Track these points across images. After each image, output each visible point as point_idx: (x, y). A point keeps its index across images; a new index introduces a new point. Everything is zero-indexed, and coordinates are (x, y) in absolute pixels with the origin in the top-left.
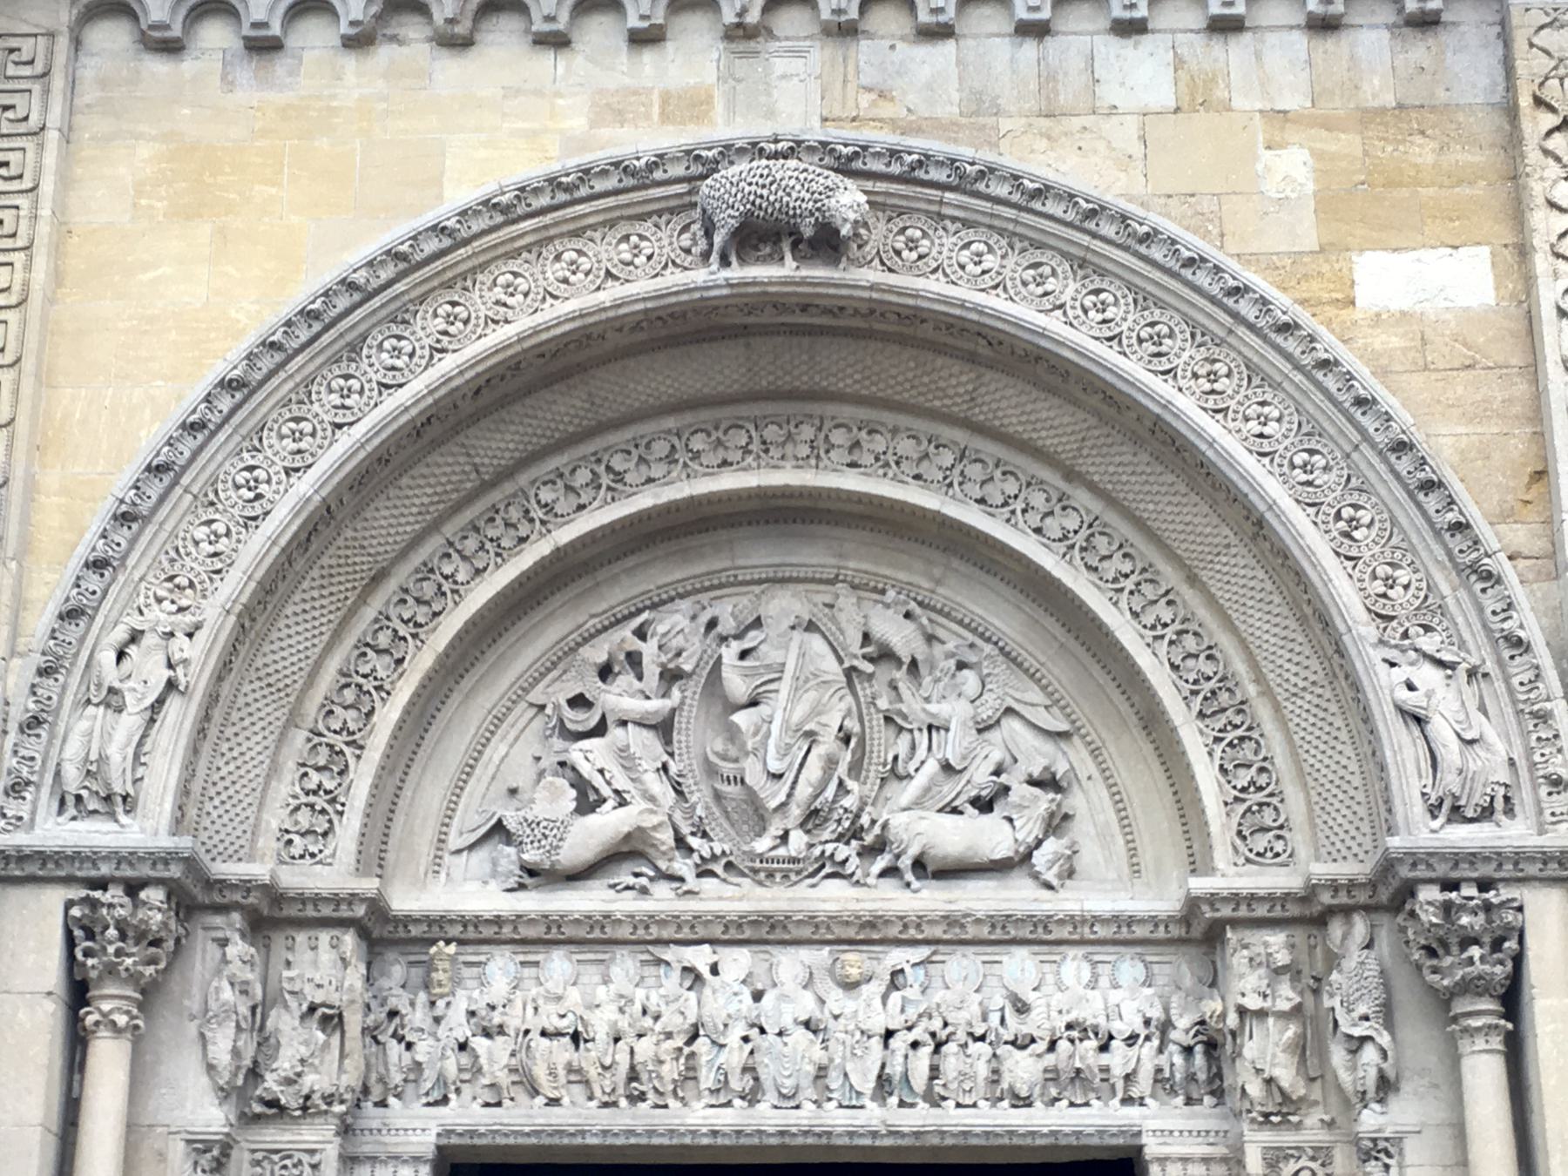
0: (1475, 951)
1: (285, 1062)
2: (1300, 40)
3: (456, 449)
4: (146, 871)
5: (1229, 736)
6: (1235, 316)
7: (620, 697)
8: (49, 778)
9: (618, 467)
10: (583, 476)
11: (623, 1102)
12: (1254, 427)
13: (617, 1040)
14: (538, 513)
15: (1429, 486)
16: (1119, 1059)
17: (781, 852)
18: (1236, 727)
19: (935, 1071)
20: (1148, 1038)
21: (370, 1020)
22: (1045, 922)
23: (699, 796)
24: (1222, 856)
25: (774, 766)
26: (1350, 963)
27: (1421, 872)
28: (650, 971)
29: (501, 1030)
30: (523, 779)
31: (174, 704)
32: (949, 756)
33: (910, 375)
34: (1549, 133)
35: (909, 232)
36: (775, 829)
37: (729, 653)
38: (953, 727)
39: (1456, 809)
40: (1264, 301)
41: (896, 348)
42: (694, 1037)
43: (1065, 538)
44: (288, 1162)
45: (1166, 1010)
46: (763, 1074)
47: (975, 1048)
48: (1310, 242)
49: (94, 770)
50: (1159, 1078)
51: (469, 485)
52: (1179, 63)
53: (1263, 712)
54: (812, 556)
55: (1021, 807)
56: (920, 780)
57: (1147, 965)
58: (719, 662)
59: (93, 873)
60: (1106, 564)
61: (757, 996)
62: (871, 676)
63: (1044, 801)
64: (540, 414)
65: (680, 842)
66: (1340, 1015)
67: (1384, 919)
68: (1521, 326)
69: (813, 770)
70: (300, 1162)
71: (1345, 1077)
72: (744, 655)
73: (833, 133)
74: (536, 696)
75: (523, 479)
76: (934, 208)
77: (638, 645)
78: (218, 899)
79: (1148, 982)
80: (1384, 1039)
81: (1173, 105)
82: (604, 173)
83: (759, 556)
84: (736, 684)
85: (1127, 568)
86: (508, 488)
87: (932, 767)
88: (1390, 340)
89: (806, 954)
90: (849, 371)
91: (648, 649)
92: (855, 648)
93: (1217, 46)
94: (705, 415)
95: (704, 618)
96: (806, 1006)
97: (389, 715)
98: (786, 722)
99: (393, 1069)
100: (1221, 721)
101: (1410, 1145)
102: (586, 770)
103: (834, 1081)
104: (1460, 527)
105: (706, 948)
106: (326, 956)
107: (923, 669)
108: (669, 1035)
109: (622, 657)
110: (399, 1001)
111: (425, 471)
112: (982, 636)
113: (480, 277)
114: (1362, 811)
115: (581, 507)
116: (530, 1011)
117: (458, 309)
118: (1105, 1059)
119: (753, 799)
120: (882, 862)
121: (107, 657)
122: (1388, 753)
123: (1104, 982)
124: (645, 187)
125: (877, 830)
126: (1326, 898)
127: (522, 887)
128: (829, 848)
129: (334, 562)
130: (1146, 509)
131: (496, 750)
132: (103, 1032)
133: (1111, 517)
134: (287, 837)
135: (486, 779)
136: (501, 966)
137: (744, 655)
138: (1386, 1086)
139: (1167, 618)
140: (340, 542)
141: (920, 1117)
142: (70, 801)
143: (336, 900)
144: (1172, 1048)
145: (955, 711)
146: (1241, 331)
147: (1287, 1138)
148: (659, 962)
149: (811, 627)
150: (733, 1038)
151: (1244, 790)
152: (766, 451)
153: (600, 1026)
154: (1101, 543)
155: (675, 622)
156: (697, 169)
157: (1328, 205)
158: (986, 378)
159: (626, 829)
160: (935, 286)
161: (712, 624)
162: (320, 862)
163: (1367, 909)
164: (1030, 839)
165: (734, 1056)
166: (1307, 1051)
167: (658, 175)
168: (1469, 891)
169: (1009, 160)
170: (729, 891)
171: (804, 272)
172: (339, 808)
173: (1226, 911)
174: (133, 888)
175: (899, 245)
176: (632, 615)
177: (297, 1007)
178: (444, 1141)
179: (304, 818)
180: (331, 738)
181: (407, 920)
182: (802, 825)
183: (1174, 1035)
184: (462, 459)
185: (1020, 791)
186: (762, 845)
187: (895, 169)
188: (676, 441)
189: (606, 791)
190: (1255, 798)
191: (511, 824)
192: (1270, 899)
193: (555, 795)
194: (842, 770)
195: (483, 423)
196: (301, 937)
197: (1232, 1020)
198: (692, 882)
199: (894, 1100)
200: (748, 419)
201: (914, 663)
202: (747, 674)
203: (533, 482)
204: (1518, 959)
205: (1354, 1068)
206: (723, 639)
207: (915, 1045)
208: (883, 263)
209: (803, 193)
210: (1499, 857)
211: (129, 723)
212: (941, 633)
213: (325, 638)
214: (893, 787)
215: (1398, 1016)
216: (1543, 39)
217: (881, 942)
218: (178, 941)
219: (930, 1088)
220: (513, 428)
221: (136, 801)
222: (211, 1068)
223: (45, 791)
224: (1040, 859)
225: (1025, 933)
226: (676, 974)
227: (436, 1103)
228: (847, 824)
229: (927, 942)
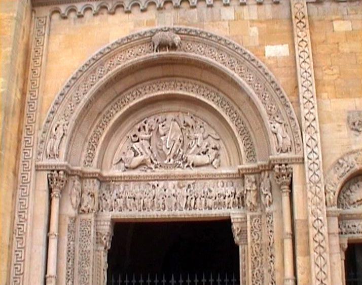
0: (284, 177)
1: (85, 204)
2: (256, 7)
5: (246, 138)
6: (244, 58)
7: (142, 135)
11: (142, 210)
12: (248, 79)
13: (141, 199)
15: (278, 89)
16: (227, 200)
17: (169, 163)
19: (195, 203)
21: (99, 196)
22: (215, 175)
23: (155, 153)
24: (244, 162)
25: (168, 147)
26: (265, 180)
28: (147, 186)
29: (122, 197)
34: (298, 23)
36: (168, 159)
37: (160, 126)
38: (199, 138)
39: (282, 150)
40: (249, 55)
42: (154, 198)
45: (235, 191)
46: (165, 204)
47: (202, 199)
48: (257, 43)
52: (235, 11)
54: (175, 107)
55: (210, 154)
56: (193, 149)
61: (165, 190)
62: (185, 129)
63: (215, 152)
65: (152, 162)
66: (263, 191)
67: (270, 172)
68: (294, 59)
72: (163, 126)
74: (128, 135)
77: (145, 125)
79: (233, 185)
80: (270, 194)
83: (165, 107)
84: (162, 132)
85: (228, 107)
87: (195, 146)
88: (271, 62)
89: (174, 182)
91: (146, 126)
92: (183, 124)
93: (241, 7)
95: (156, 120)
96: (173, 191)
98: (170, 138)
101: (274, 214)
102: (135, 148)
103: (178, 206)
104: (283, 97)
106: (91, 184)
107: (194, 127)
108: (150, 198)
110: (105, 192)
118: (224, 200)
119: (164, 152)
120: (186, 165)
126: (261, 168)
127: (125, 171)
130: (232, 95)
131: (121, 145)
132: (54, 197)
133: (226, 97)
136: (122, 185)
137: (163, 126)
138: (270, 203)
139: (235, 116)
141: (193, 212)
145: (199, 135)
146: (246, 61)
147: (254, 214)
148: (148, 184)
149: (175, 120)
150: (161, 198)
153: (138, 195)
154: (224, 103)
155: (151, 121)
157: (261, 37)
159: (142, 159)
160: (193, 54)
161: (158, 120)
163: (268, 170)
165: (161, 201)
166: (258, 197)
168: (283, 166)
170: (160, 170)
173: (244, 172)
176: (144, 119)
177: (87, 193)
178: (112, 217)
179: (88, 159)
181: (106, 177)
183: (237, 196)
185: (210, 150)
186: (166, 162)
189: (139, 152)
191: (123, 159)
193: (130, 153)
196: (88, 180)
197: (245, 192)
198: (154, 169)
204: (292, 178)
206: (160, 123)
207: (192, 198)
210: (288, 159)
215: (273, 190)
216: (296, 6)
217: (187, 179)
218: (66, 181)
219: (194, 206)
222: (72, 204)
224: (214, 163)
225: (211, 177)
228: (180, 157)
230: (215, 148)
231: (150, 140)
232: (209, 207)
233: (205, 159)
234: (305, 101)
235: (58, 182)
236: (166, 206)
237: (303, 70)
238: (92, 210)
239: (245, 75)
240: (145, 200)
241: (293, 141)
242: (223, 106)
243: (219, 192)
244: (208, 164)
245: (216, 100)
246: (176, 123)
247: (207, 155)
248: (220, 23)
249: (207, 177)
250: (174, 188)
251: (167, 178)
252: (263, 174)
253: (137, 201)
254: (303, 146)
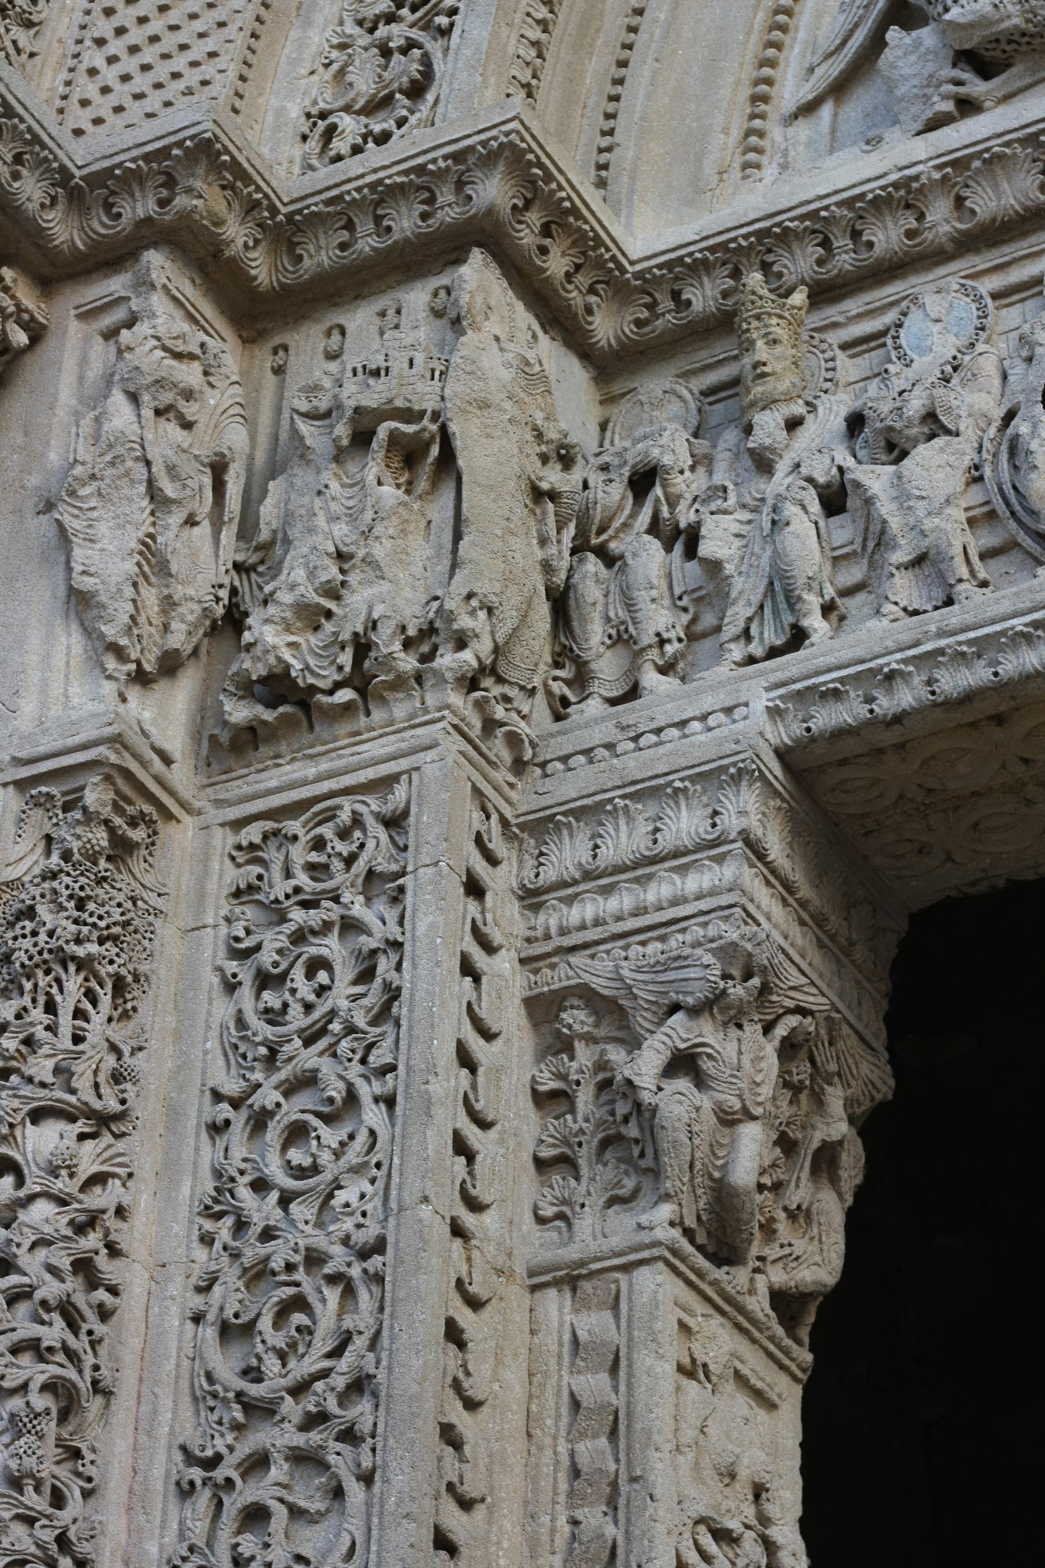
44: (327, 831)
70: (357, 821)
78: (100, 225)
127: (967, 106)
134: (322, 125)
172: (443, 20)
227: (773, 653)
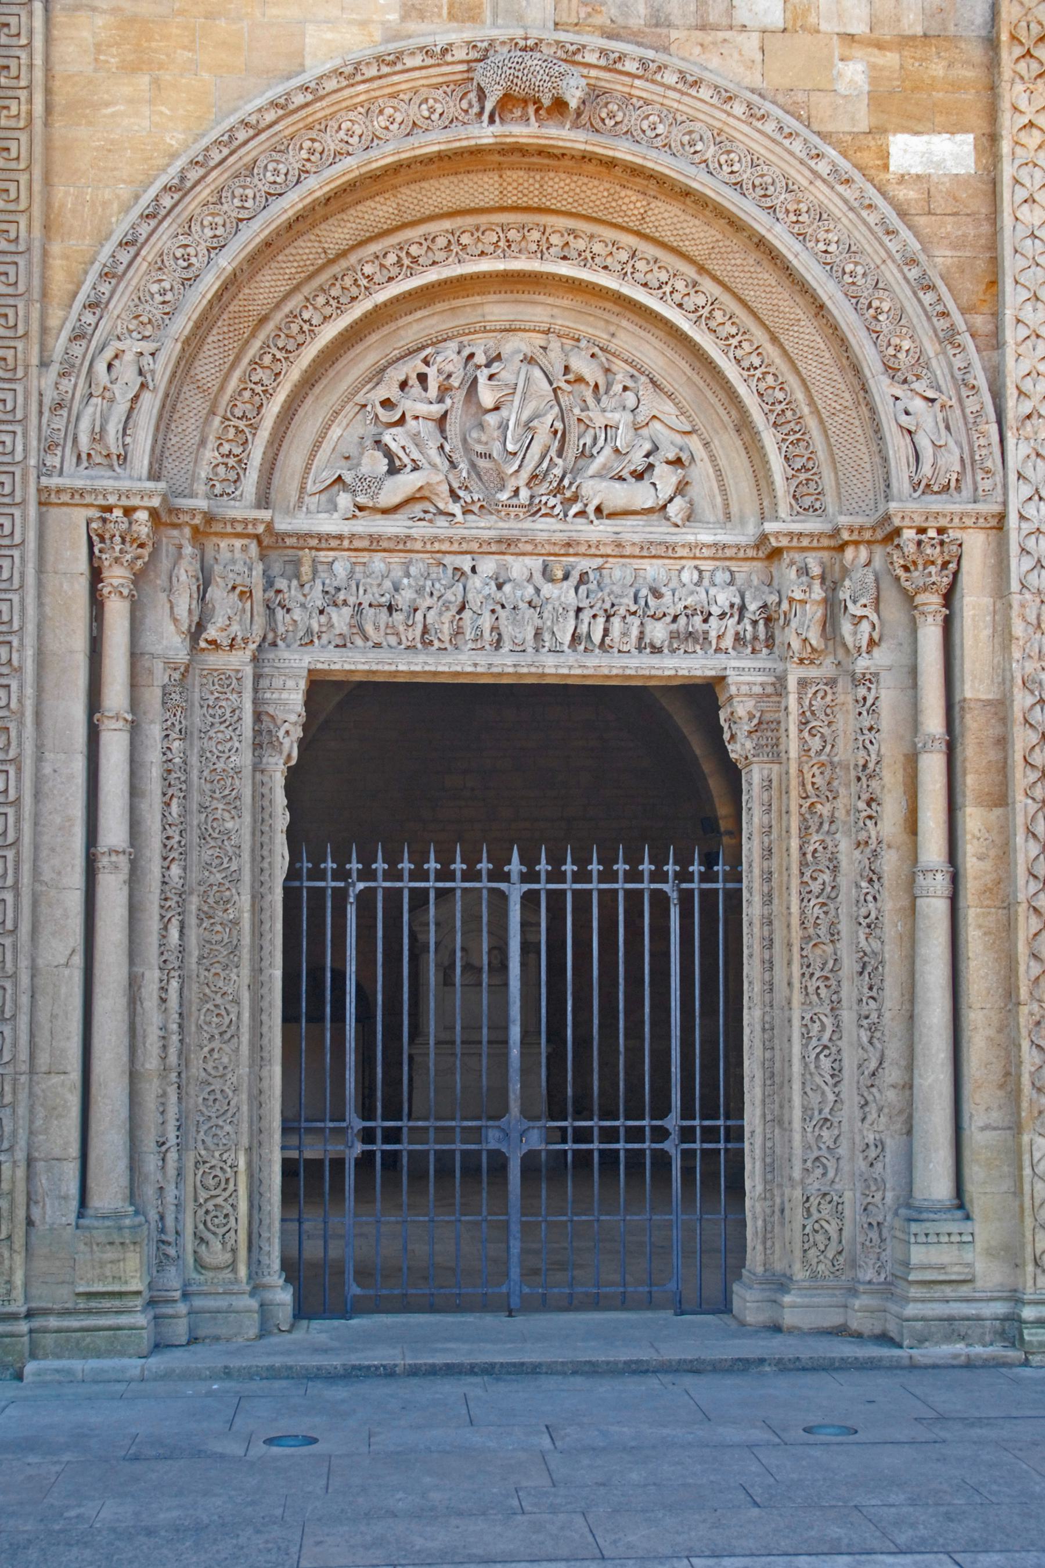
0: (932, 569)
1: (220, 620)
3: (313, 237)
4: (135, 501)
5: (791, 438)
8: (69, 444)
9: (414, 254)
10: (392, 258)
13: (416, 610)
14: (364, 282)
17: (514, 501)
18: (796, 432)
19: (606, 632)
20: (732, 615)
24: (783, 511)
25: (510, 447)
27: (907, 522)
28: (434, 569)
30: (353, 451)
31: (147, 396)
32: (618, 444)
33: (604, 200)
35: (610, 106)
41: (596, 183)
42: (462, 609)
43: (696, 310)
47: (629, 619)
49: (98, 436)
50: (738, 638)
51: (320, 262)
53: (812, 423)
57: (732, 573)
58: (475, 380)
59: (103, 503)
60: (720, 328)
61: (499, 587)
64: (366, 216)
65: (452, 492)
66: (849, 604)
69: (536, 450)
71: (849, 640)
73: (562, 36)
74: (360, 399)
75: (353, 259)
76: (627, 90)
77: (425, 369)
80: (874, 617)
81: (781, 26)
82: (413, 54)
84: (487, 397)
86: (344, 264)
87: (608, 451)
89: (528, 560)
90: (565, 196)
91: (431, 372)
94: (470, 221)
95: (466, 353)
97: (273, 408)
98: (517, 420)
99: (280, 624)
100: (786, 429)
102: (394, 446)
103: (547, 636)
105: (469, 557)
107: (602, 389)
108: (448, 609)
109: (414, 376)
111: (294, 251)
112: (639, 370)
113: (330, 123)
114: (869, 485)
115: (390, 279)
116: (361, 591)
117: (316, 145)
118: (705, 627)
121: (101, 367)
122: (891, 452)
123: (706, 582)
124: (439, 65)
125: (573, 489)
126: (846, 536)
128: (544, 499)
129: (236, 309)
131: (335, 432)
135: (329, 451)
137: (491, 377)
140: (241, 296)
142: (84, 456)
143: (245, 522)
144: (746, 621)
148: (440, 564)
149: (530, 360)
150: (487, 614)
151: (798, 470)
152: (509, 246)
154: (718, 314)
156: (474, 55)
158: (652, 206)
159: (419, 484)
161: (471, 356)
162: (234, 499)
163: (869, 543)
164: (667, 497)
165: (486, 622)
166: (830, 625)
167: (449, 58)
168: (932, 533)
169: (675, 62)
171: (543, 130)
173: (784, 542)
174: (128, 511)
175: (604, 115)
180: (235, 422)
182: (527, 484)
183: (748, 615)
184: (316, 244)
187: (603, 62)
188: (450, 237)
189: (406, 460)
190: (803, 476)
191: (348, 477)
192: (811, 535)
194: (553, 453)
195: (331, 221)
196: (223, 544)
199: (582, 647)
200: (497, 225)
201: (596, 386)
202: (493, 388)
203: (360, 261)
204: (956, 574)
205: (855, 633)
206: (478, 367)
207: (594, 616)
208: (592, 125)
209: (545, 77)
211: (121, 408)
212: (614, 368)
213: (231, 358)
214: (581, 462)
215: (882, 606)
217: (576, 555)
220: (349, 225)
221: (125, 458)
223: (68, 450)
224: (672, 510)
225: (661, 551)
226: (450, 571)
228: (555, 484)
229: (602, 556)
230: (678, 462)
231: (442, 421)
232: (653, 646)
233: (642, 496)
234: (1023, 332)
235: (127, 547)
236: (505, 637)
237: (1022, 231)
238: (246, 641)
239: (810, 231)
240: (431, 616)
241: (968, 461)
242: (713, 324)
243: (689, 601)
244: (650, 511)
245: (689, 304)
246: (537, 373)
247: (646, 483)
248: (728, 35)
249: (645, 553)
250: (530, 579)
251: (507, 545)
252: (849, 553)
253: (398, 617)
254: (1005, 476)
